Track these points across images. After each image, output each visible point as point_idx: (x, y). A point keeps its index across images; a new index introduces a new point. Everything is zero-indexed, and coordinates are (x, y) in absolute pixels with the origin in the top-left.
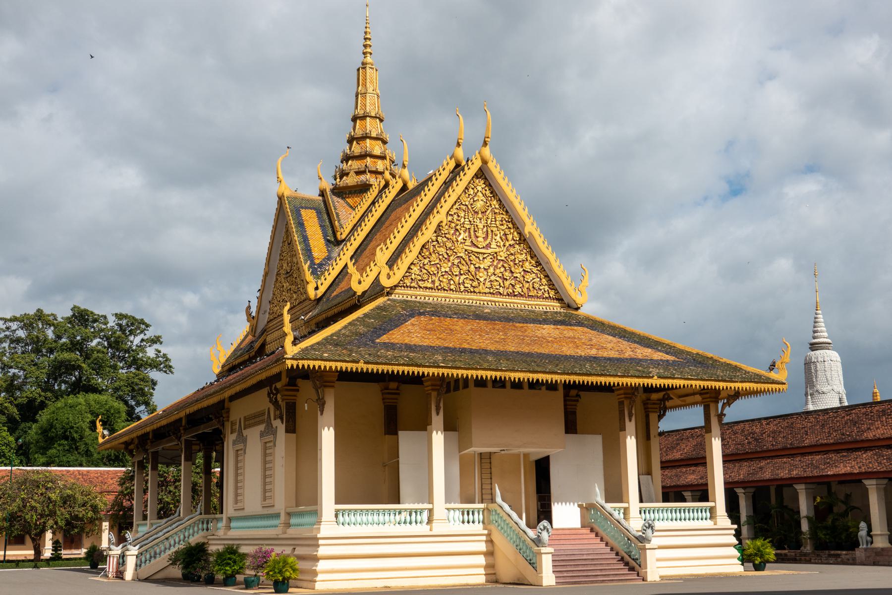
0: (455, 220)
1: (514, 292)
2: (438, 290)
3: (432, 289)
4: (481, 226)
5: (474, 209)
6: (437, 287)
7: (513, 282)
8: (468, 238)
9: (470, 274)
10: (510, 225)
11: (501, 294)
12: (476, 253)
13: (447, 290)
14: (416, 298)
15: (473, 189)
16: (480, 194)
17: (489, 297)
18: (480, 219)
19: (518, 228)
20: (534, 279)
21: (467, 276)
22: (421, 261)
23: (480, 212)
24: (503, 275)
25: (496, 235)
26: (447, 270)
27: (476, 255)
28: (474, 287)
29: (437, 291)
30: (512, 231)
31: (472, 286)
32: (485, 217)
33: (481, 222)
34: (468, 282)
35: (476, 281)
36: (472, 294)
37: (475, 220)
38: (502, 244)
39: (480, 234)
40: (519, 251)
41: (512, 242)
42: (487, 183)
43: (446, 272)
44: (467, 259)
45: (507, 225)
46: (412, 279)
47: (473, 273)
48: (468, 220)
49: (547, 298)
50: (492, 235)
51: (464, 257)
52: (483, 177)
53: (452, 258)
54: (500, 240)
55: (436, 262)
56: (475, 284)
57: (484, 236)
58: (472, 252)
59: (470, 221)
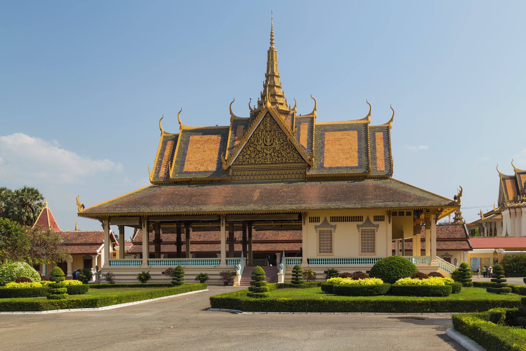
0: (257, 136)
2: (251, 164)
4: (269, 137)
6: (250, 163)
11: (277, 163)
15: (265, 122)
16: (268, 124)
21: (263, 158)
23: (268, 131)
24: (278, 156)
25: (275, 140)
26: (254, 156)
27: (266, 149)
28: (265, 162)
38: (278, 143)
39: (268, 140)
41: (283, 141)
42: (272, 119)
43: (253, 157)
44: (262, 151)
46: (239, 161)
49: (297, 163)
52: (270, 116)
54: (277, 142)
56: (265, 160)
57: (270, 140)
59: (264, 135)
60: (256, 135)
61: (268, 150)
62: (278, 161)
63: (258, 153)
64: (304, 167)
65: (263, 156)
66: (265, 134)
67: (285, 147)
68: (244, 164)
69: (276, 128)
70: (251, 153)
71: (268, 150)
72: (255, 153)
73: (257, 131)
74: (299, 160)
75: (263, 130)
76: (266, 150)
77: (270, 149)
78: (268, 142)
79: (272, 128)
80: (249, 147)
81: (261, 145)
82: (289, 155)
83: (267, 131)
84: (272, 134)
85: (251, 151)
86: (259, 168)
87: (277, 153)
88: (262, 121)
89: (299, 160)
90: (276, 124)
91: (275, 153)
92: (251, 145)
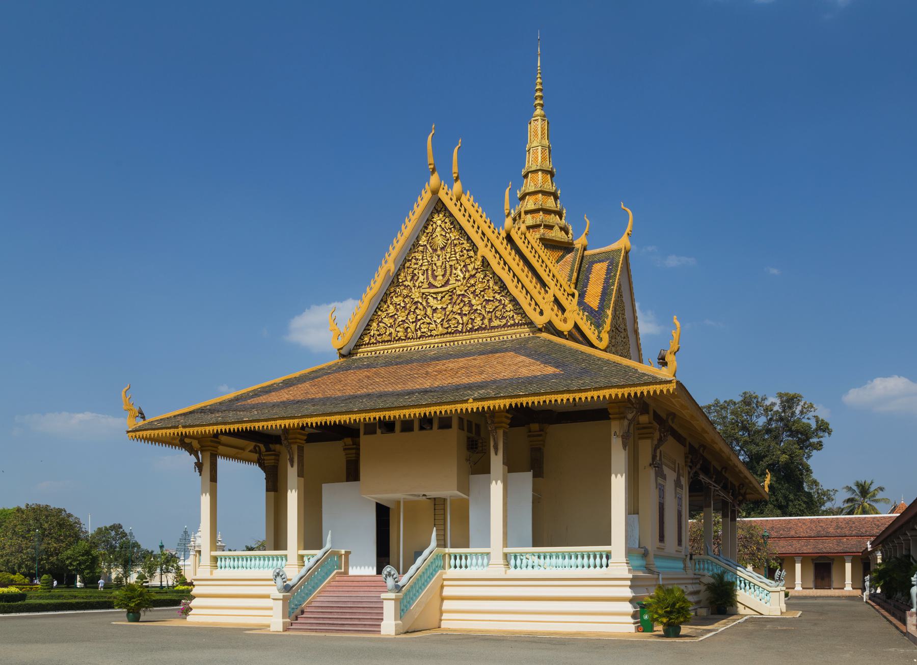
2: (396, 341)
4: (439, 263)
6: (394, 338)
8: (425, 280)
9: (427, 318)
12: (434, 293)
13: (405, 340)
14: (376, 353)
16: (439, 229)
17: (447, 337)
18: (439, 256)
20: (497, 307)
23: (439, 249)
24: (462, 311)
25: (456, 269)
26: (404, 319)
27: (435, 296)
28: (431, 330)
29: (395, 342)
32: (443, 252)
33: (438, 260)
34: (425, 326)
35: (433, 323)
36: (430, 338)
38: (462, 276)
39: (439, 272)
40: (481, 280)
41: (474, 272)
42: (447, 214)
43: (402, 321)
44: (424, 303)
47: (431, 316)
49: (512, 325)
50: (451, 270)
51: (421, 301)
52: (443, 209)
53: (408, 306)
55: (393, 314)
57: (443, 273)
61: (439, 298)
62: (462, 324)
67: (479, 287)
70: (397, 311)
75: (427, 248)
77: (444, 294)
78: (438, 278)
82: (490, 307)
84: (448, 255)
87: (459, 304)
90: (458, 227)
91: (455, 303)
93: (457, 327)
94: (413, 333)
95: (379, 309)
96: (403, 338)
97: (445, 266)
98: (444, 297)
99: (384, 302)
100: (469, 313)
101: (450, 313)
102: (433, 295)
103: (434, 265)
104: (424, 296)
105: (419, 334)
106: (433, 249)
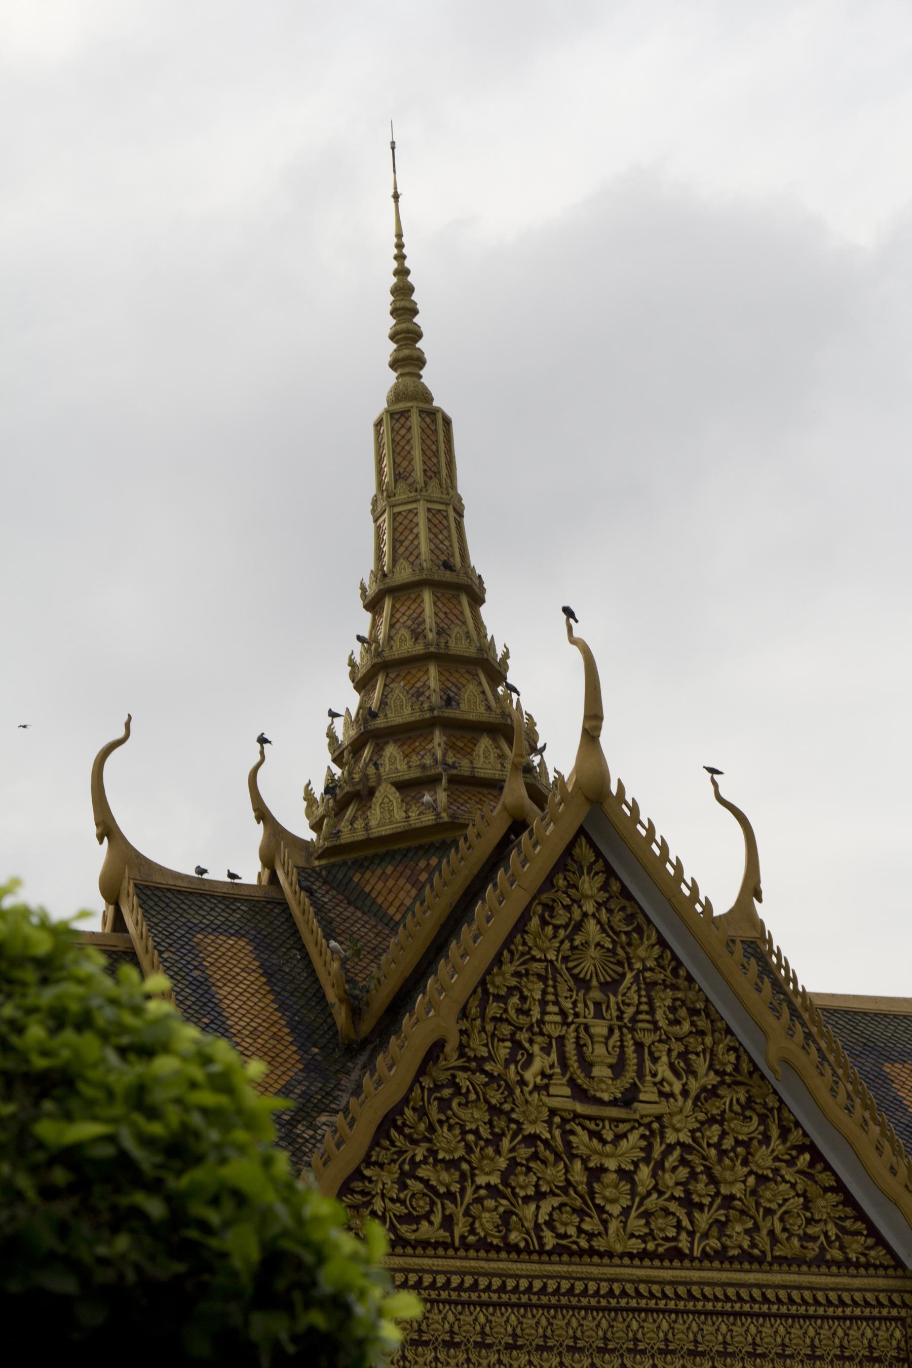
0: (512, 1013)
1: (725, 1247)
2: (467, 1247)
3: (446, 1246)
4: (600, 1029)
5: (576, 971)
6: (463, 1238)
7: (721, 1215)
8: (558, 1070)
9: (571, 1192)
10: (702, 1023)
15: (568, 908)
19: (729, 1031)
21: (564, 1199)
22: (401, 1152)
24: (688, 1192)
25: (655, 1060)
26: (495, 1180)
27: (592, 1126)
28: (591, 1236)
30: (708, 1040)
31: (580, 1231)
32: (612, 998)
35: (594, 1214)
37: (580, 1006)
40: (736, 1108)
42: (615, 887)
43: (488, 1186)
45: (693, 1023)
48: (555, 1009)
49: (838, 1264)
52: (599, 866)
53: (506, 1144)
54: (669, 1075)
57: (613, 1060)
58: (576, 1116)
59: (563, 1013)
60: (498, 998)
62: (691, 1234)
63: (524, 1152)
64: (893, 1304)
65: (568, 1182)
66: (575, 1004)
68: (415, 1245)
69: (650, 963)
71: (604, 1142)
72: (498, 1152)
73: (509, 968)
74: (855, 1247)
75: (555, 970)
76: (584, 1135)
77: (623, 1128)
78: (596, 1071)
79: (620, 963)
80: (446, 1092)
81: (546, 1087)
83: (582, 983)
84: (630, 1011)
85: (464, 1132)
86: (537, 1285)
87: (674, 1169)
88: (545, 898)
89: (847, 1239)
91: (660, 1165)
92: (462, 1079)
93: (674, 1239)
94: (528, 1233)
95: (400, 1130)
96: (495, 1241)
97: (622, 1041)
98: (624, 1136)
99: (414, 1109)
100: (711, 1205)
101: (649, 1194)
102: (587, 1123)
103: (582, 1027)
104: (557, 1120)
105: (550, 1240)
106: (575, 977)
